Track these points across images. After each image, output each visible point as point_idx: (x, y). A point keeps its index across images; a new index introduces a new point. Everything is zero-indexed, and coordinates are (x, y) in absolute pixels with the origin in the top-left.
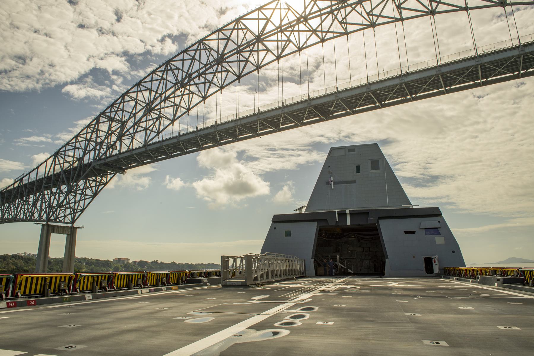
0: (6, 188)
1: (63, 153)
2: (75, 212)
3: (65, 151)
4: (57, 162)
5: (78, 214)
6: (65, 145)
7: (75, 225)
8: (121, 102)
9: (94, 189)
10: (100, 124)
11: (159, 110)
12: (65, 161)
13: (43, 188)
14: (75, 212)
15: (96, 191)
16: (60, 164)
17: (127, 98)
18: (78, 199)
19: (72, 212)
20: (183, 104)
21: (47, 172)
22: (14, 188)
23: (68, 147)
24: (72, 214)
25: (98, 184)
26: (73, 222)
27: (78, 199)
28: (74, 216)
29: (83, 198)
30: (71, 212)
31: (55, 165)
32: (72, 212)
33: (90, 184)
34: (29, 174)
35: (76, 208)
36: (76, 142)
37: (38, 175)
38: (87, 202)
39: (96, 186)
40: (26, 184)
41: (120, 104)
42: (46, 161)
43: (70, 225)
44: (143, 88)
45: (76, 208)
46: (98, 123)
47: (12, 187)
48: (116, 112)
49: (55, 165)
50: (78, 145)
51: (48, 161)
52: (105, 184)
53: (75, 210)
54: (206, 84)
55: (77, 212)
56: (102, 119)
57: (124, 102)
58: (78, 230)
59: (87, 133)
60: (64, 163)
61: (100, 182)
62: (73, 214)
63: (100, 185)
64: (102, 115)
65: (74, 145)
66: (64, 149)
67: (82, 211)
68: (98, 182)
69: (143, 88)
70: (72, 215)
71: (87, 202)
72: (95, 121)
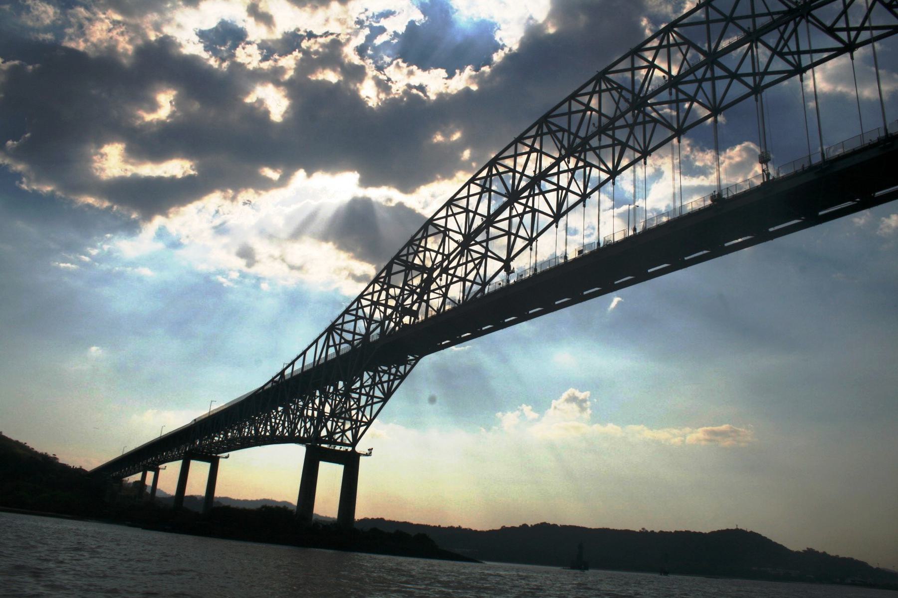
1: (340, 327)
2: (358, 425)
3: (343, 323)
4: (331, 343)
5: (362, 429)
6: (343, 315)
7: (359, 448)
9: (385, 385)
10: (392, 277)
11: (484, 244)
12: (343, 341)
14: (358, 425)
15: (389, 388)
16: (335, 345)
18: (363, 403)
19: (354, 426)
20: (522, 232)
21: (317, 358)
24: (354, 428)
25: (392, 377)
26: (356, 440)
27: (363, 403)
28: (357, 432)
29: (370, 402)
30: (352, 425)
32: (354, 426)
34: (293, 363)
35: (360, 419)
36: (357, 309)
38: (376, 407)
39: (388, 382)
42: (316, 341)
43: (350, 449)
45: (360, 419)
46: (389, 274)
49: (329, 347)
50: (360, 313)
51: (296, 363)
56: (396, 268)
58: (362, 458)
59: (372, 294)
60: (340, 344)
61: (395, 375)
63: (394, 379)
64: (396, 261)
65: (354, 312)
66: (340, 321)
68: (392, 374)
72: (385, 272)
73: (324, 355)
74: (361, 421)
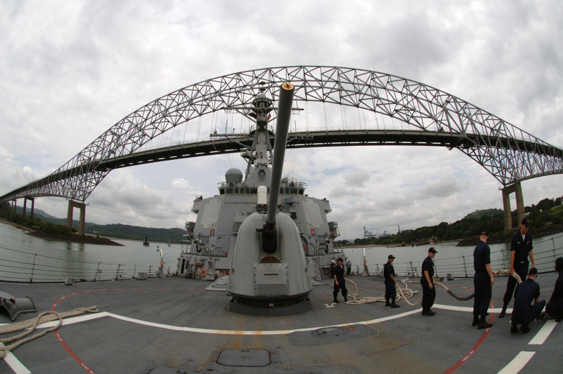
0: (52, 174)
3: (85, 152)
4: (79, 160)
5: (87, 195)
6: (85, 149)
10: (107, 136)
13: (70, 176)
15: (98, 181)
17: (126, 121)
19: (84, 194)
21: (73, 165)
22: (56, 174)
23: (87, 150)
25: (99, 176)
26: (84, 201)
28: (85, 197)
29: (90, 185)
31: (78, 161)
33: (95, 177)
34: (64, 166)
37: (68, 167)
38: (93, 187)
41: (121, 124)
42: (73, 158)
44: (137, 115)
46: (106, 135)
48: (118, 129)
49: (78, 161)
52: (104, 177)
54: (165, 123)
55: (86, 194)
56: (109, 133)
57: (124, 123)
61: (101, 175)
64: (109, 131)
67: (90, 193)
69: (137, 115)
71: (93, 187)
73: (76, 164)
74: (87, 192)
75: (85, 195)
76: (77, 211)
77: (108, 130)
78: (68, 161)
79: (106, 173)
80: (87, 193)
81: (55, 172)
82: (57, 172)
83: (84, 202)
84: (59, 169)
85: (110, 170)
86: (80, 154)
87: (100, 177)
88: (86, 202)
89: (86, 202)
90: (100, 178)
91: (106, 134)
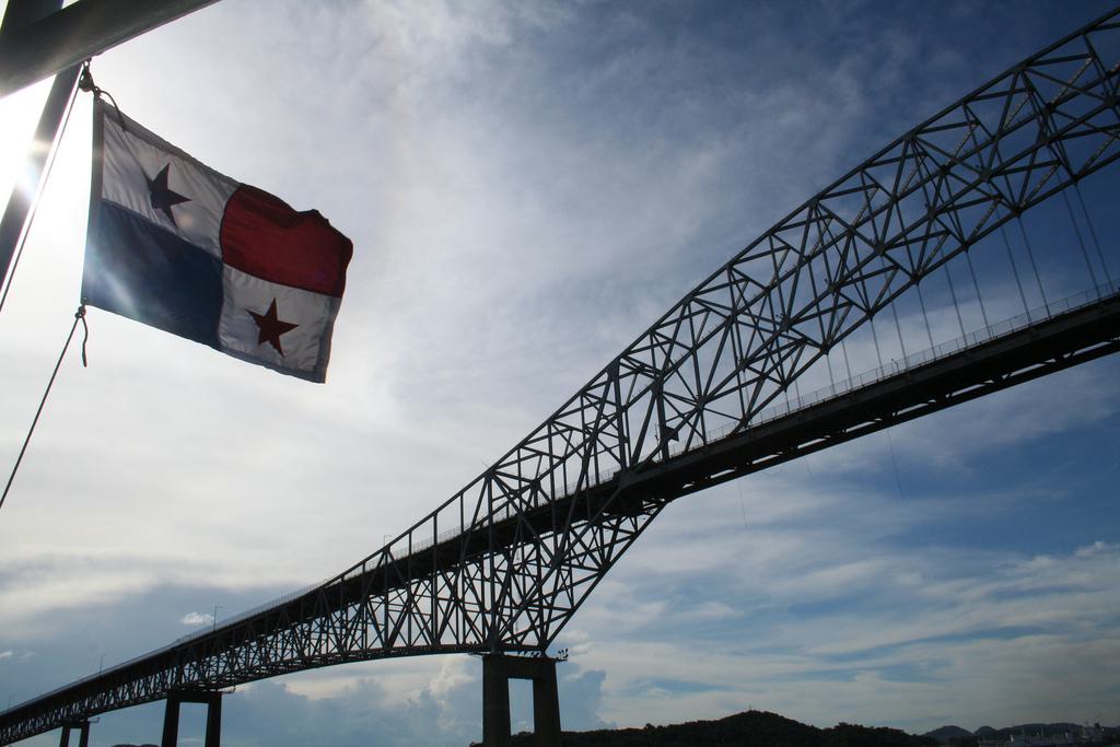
0: (342, 576)
2: (545, 619)
5: (553, 626)
8: (683, 317)
14: (545, 619)
17: (695, 307)
19: (537, 623)
22: (365, 574)
23: (524, 453)
24: (538, 626)
28: (544, 634)
30: (533, 622)
31: (491, 501)
32: (537, 623)
38: (579, 591)
40: (404, 559)
41: (678, 322)
47: (359, 571)
52: (633, 536)
53: (546, 612)
56: (623, 371)
62: (541, 626)
64: (623, 361)
67: (570, 613)
70: (539, 630)
71: (579, 591)
75: (545, 625)
76: (521, 693)
77: (619, 358)
78: (433, 510)
79: (642, 519)
80: (555, 614)
81: (363, 563)
82: (372, 565)
83: (543, 653)
84: (386, 550)
85: (661, 506)
86: (491, 474)
87: (614, 541)
88: (551, 652)
89: (551, 652)
90: (611, 546)
91: (612, 370)
